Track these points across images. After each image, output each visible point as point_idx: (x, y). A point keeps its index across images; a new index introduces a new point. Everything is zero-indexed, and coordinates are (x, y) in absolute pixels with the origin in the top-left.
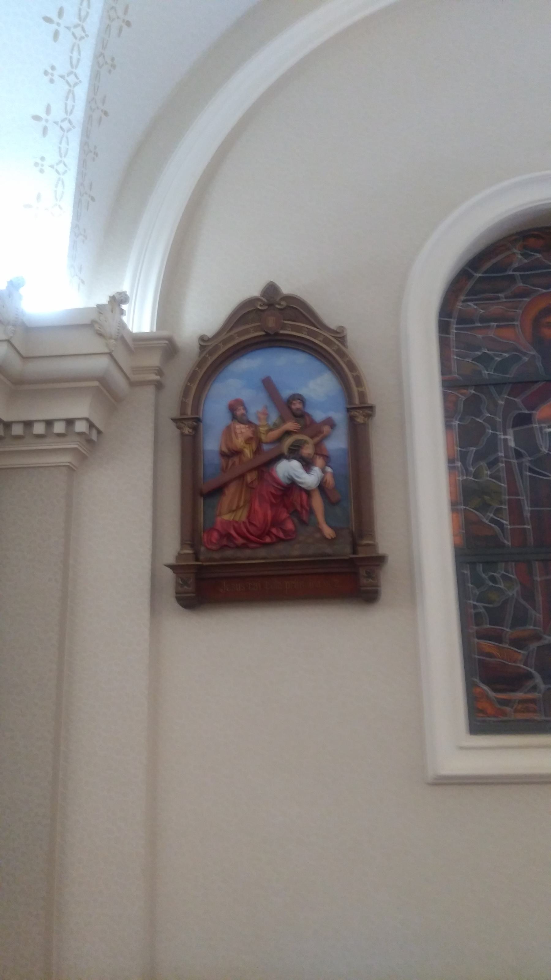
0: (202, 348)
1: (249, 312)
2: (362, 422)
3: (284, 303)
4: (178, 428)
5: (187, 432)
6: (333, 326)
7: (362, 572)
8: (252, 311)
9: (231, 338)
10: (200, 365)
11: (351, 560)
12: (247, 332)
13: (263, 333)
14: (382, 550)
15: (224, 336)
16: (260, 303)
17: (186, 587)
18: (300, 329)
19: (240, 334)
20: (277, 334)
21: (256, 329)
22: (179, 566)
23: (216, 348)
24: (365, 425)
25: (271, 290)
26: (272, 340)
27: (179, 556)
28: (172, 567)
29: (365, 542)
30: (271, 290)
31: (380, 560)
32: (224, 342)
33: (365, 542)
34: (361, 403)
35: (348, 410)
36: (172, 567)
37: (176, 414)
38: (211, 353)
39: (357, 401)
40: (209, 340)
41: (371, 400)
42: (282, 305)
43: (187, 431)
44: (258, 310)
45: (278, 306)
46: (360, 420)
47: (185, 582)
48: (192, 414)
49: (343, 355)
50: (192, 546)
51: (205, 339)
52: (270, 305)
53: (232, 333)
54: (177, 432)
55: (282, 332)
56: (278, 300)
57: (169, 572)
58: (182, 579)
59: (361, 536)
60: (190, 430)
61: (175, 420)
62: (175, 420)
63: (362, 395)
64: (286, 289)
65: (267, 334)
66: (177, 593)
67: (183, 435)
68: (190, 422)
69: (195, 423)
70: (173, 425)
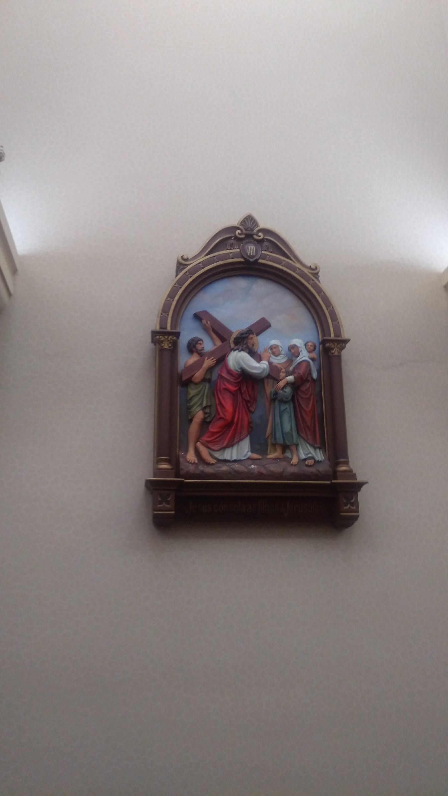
1: (229, 238)
2: (336, 354)
5: (166, 347)
6: (308, 262)
8: (232, 237)
10: (180, 283)
13: (242, 260)
15: (202, 259)
17: (164, 504)
18: (279, 262)
19: (220, 258)
25: (249, 221)
27: (157, 472)
30: (249, 221)
32: (205, 263)
33: (343, 468)
34: (335, 336)
38: (192, 272)
40: (187, 260)
41: (345, 335)
42: (260, 236)
43: (166, 346)
44: (236, 238)
45: (255, 237)
48: (171, 329)
49: (319, 290)
50: (168, 461)
55: (261, 261)
56: (255, 231)
59: (337, 464)
65: (247, 262)
67: (162, 350)
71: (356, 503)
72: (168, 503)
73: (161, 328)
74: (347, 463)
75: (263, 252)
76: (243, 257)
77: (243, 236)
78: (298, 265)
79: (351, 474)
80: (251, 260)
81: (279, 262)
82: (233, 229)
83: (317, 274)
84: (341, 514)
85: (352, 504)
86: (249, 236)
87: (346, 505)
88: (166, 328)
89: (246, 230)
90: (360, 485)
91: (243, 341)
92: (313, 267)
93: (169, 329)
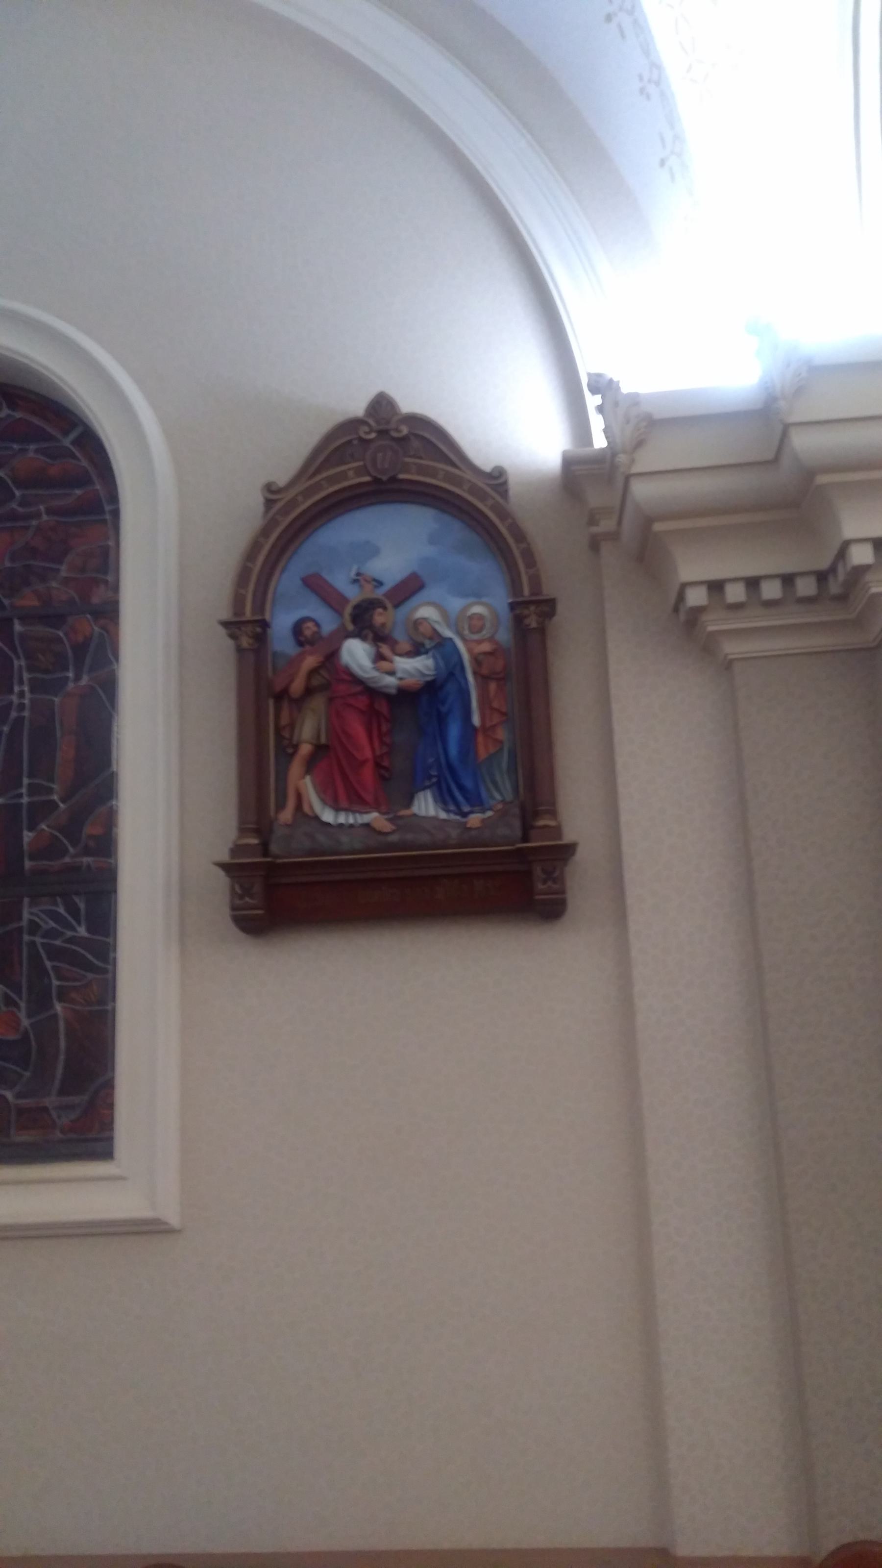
0: (269, 503)
2: (534, 625)
3: (405, 430)
4: (233, 636)
7: (538, 871)
9: (317, 487)
10: (265, 532)
11: (520, 853)
12: (343, 476)
14: (568, 837)
16: (366, 429)
17: (247, 899)
19: (331, 480)
20: (393, 479)
21: (359, 472)
22: (237, 864)
23: (292, 504)
24: (542, 631)
25: (381, 405)
26: (385, 490)
27: (236, 850)
28: (225, 867)
29: (541, 823)
30: (381, 405)
31: (567, 851)
32: (307, 493)
34: (532, 594)
35: (512, 606)
36: (225, 867)
37: (226, 614)
38: (285, 511)
39: (526, 591)
40: (279, 491)
41: (548, 590)
43: (245, 642)
44: (361, 440)
46: (532, 622)
47: (247, 892)
51: (274, 488)
52: (383, 433)
53: (318, 478)
54: (230, 643)
55: (401, 476)
57: (221, 873)
58: (241, 886)
59: (536, 814)
60: (251, 641)
61: (226, 624)
62: (226, 624)
63: (536, 582)
64: (407, 405)
65: (376, 481)
66: (234, 908)
67: (240, 650)
68: (249, 629)
69: (258, 630)
70: (222, 631)
71: (560, 880)
72: (251, 896)
73: (236, 614)
74: (553, 813)
75: (407, 460)
76: (370, 475)
77: (373, 435)
78: (468, 475)
79: (557, 831)
80: (384, 478)
81: (434, 473)
82: (352, 424)
83: (505, 483)
84: (537, 897)
85: (555, 881)
86: (383, 433)
87: (545, 882)
88: (244, 614)
89: (378, 422)
90: (570, 849)
91: (362, 621)
92: (496, 474)
93: (248, 615)
